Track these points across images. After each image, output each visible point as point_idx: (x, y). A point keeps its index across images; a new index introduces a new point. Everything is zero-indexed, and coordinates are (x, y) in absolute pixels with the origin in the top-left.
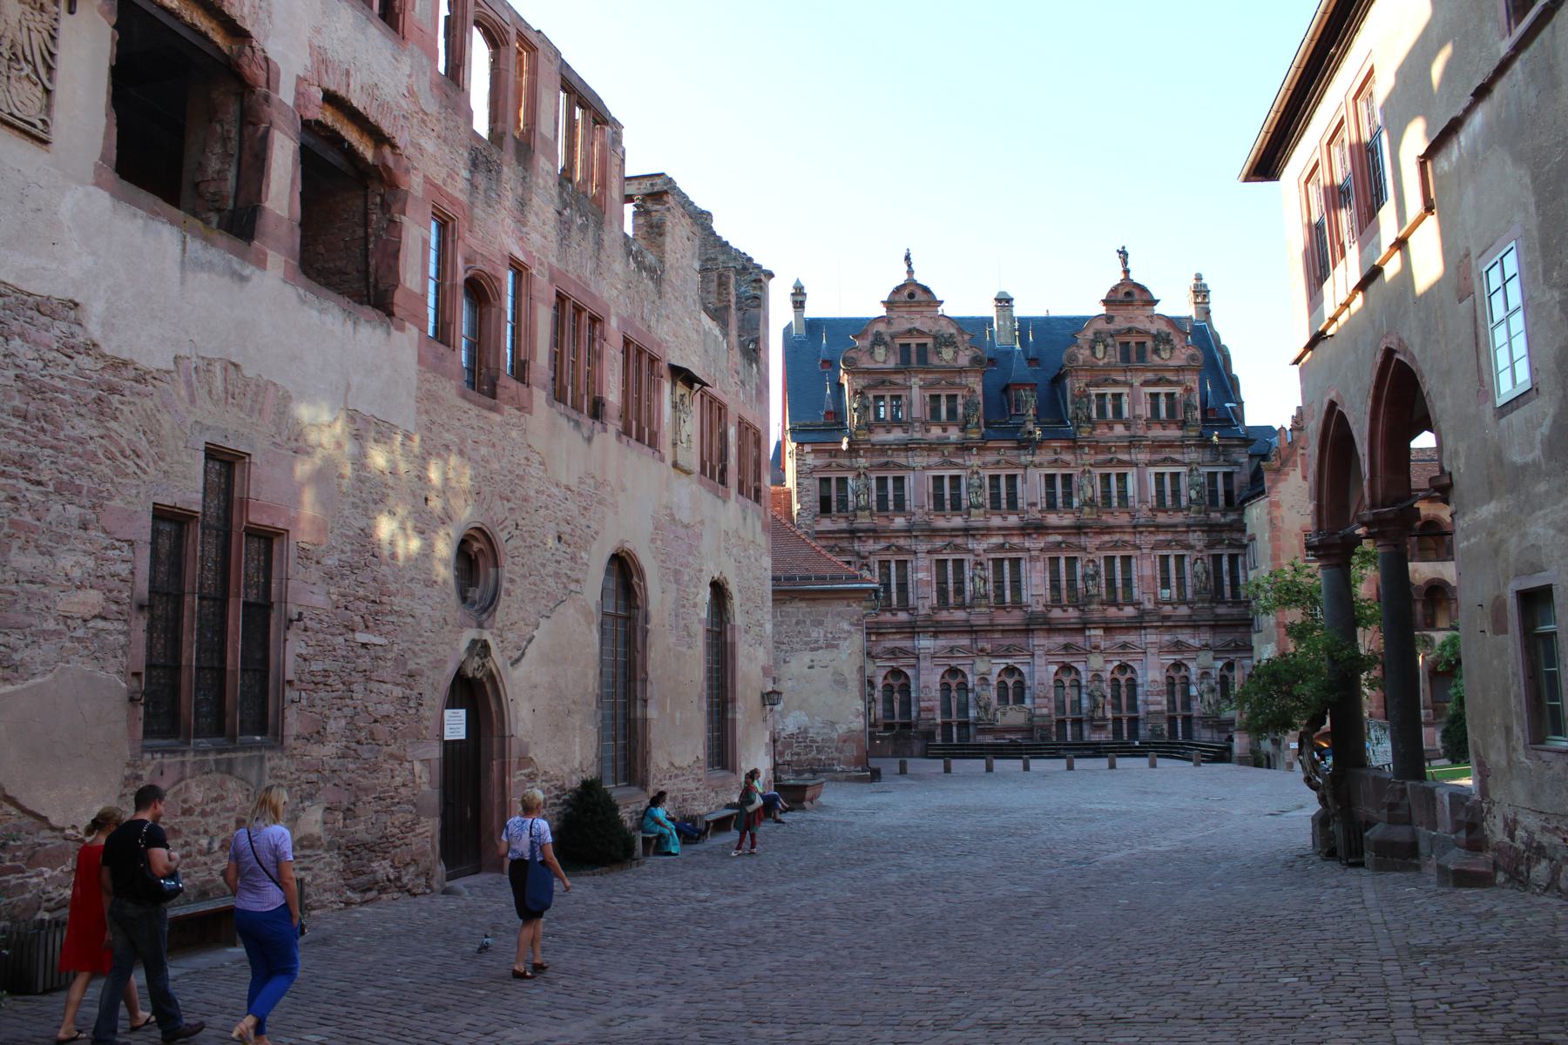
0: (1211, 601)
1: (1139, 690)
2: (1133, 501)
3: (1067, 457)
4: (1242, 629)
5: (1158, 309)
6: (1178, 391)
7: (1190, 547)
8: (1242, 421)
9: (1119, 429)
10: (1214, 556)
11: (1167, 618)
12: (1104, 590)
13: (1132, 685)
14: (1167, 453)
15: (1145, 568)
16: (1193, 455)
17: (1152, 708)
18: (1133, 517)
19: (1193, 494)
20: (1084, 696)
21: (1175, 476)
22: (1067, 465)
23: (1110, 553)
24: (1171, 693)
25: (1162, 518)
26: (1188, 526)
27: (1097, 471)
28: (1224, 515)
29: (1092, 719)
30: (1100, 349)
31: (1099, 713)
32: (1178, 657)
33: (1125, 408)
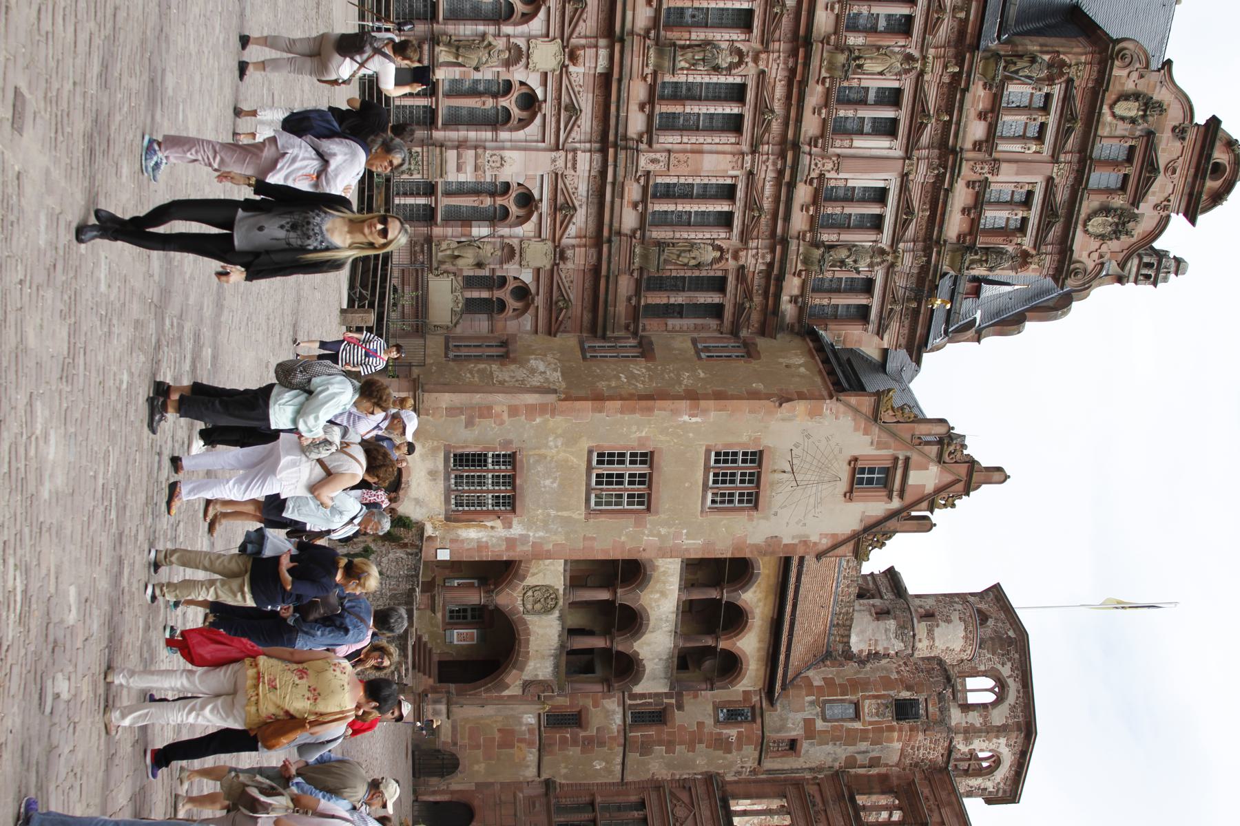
0: (641, 269)
1: (489, 135)
2: (839, 146)
3: (945, 30)
4: (587, 317)
5: (1178, 221)
6: (1027, 242)
7: (745, 236)
8: (951, 341)
9: (976, 130)
10: (723, 280)
11: (619, 191)
12: (681, 78)
13: (500, 120)
14: (921, 213)
15: (716, 161)
16: (908, 262)
17: (451, 155)
18: (813, 142)
19: (843, 254)
20: (481, 28)
21: (876, 223)
22: (931, 26)
23: (750, 95)
24: (475, 190)
25: (803, 193)
26: (785, 242)
27: (907, 84)
28: (794, 300)
29: (434, 40)
30: (1129, 109)
31: (443, 55)
32: (545, 207)
33: (1017, 147)
